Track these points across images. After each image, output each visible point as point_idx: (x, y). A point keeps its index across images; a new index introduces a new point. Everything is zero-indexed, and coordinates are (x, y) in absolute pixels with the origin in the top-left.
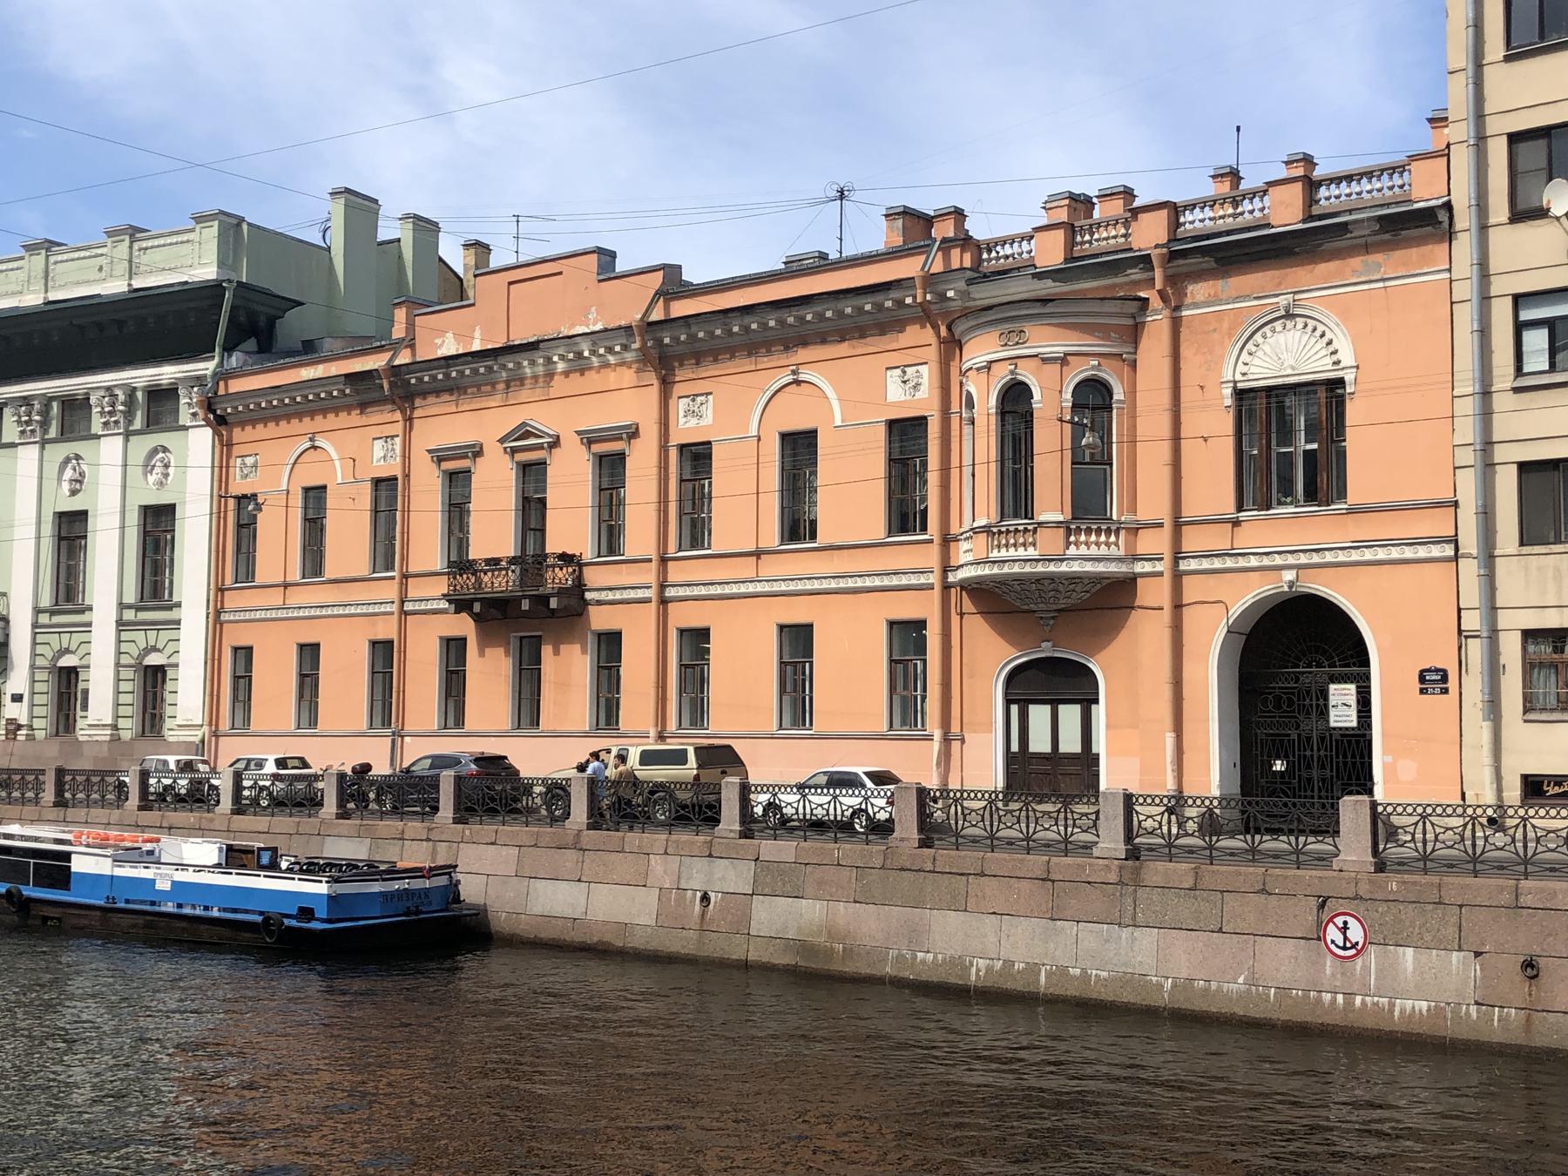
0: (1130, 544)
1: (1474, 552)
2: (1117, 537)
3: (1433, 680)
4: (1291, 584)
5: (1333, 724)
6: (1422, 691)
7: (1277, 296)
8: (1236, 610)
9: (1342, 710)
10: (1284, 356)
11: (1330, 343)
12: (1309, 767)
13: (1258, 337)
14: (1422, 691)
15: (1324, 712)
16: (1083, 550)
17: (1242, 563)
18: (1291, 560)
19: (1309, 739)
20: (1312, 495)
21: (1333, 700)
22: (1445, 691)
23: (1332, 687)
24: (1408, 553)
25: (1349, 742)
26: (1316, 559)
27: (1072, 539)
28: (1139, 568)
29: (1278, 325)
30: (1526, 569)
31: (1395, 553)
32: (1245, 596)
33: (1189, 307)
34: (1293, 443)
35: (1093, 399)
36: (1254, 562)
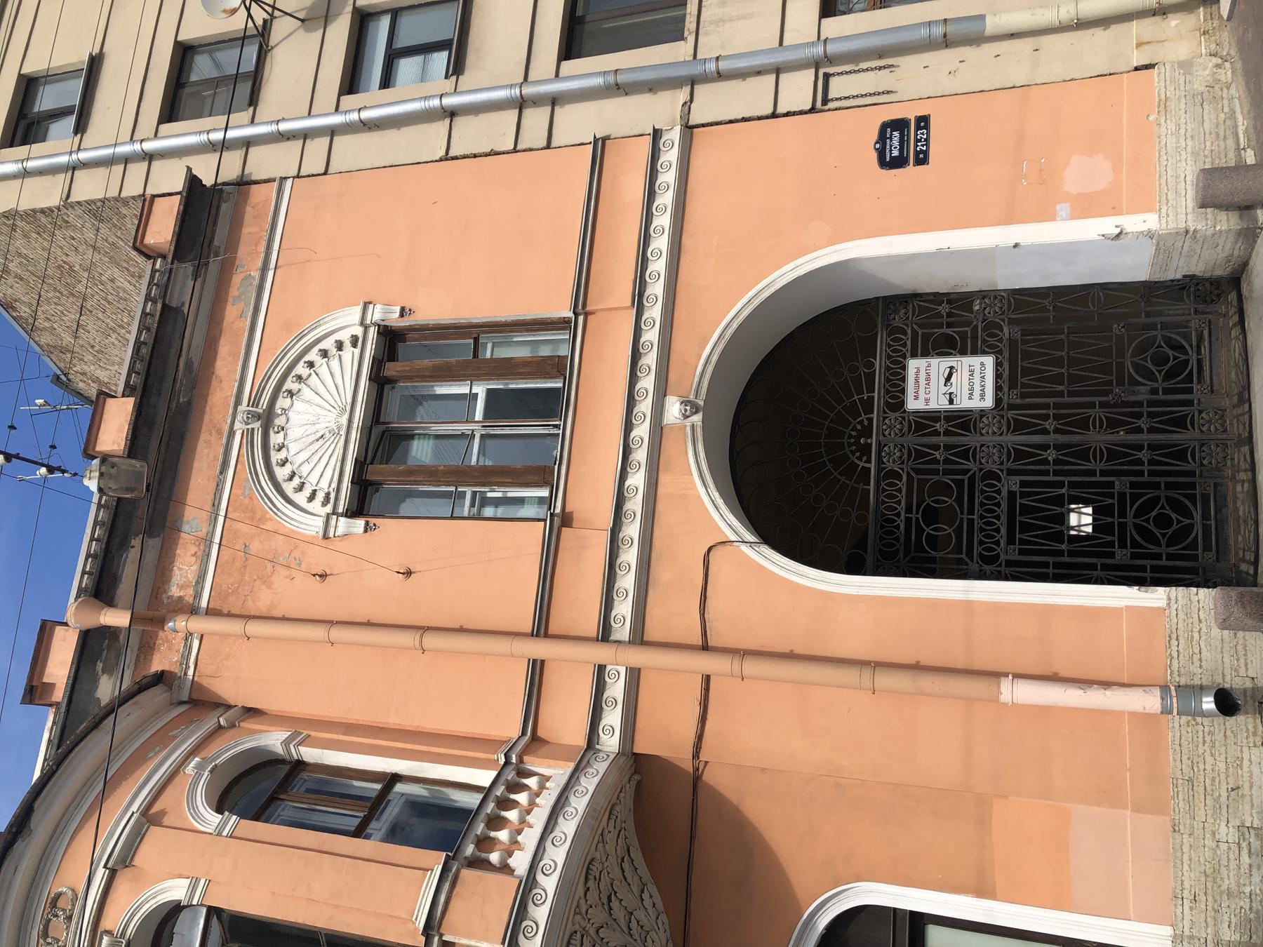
0: (560, 753)
1: (682, 95)
2: (530, 774)
3: (902, 144)
4: (691, 407)
5: (989, 403)
6: (922, 159)
7: (232, 433)
8: (725, 522)
9: (960, 382)
10: (320, 422)
11: (324, 354)
12: (1083, 454)
13: (281, 473)
14: (922, 159)
15: (963, 421)
16: (529, 839)
17: (635, 505)
18: (645, 406)
19: (1020, 455)
20: (549, 405)
21: (938, 402)
22: (923, 122)
23: (912, 404)
24: (665, 199)
25: (1026, 372)
26: (650, 359)
27: (494, 857)
28: (610, 742)
29: (276, 439)
30: (720, 21)
31: (663, 221)
32: (704, 508)
33: (198, 595)
34: (453, 415)
35: (264, 789)
36: (637, 480)
